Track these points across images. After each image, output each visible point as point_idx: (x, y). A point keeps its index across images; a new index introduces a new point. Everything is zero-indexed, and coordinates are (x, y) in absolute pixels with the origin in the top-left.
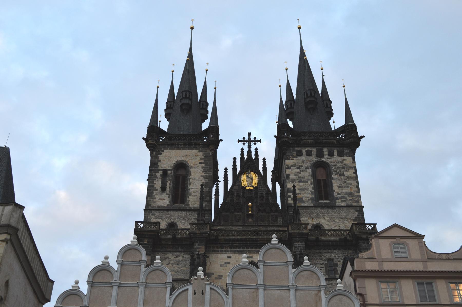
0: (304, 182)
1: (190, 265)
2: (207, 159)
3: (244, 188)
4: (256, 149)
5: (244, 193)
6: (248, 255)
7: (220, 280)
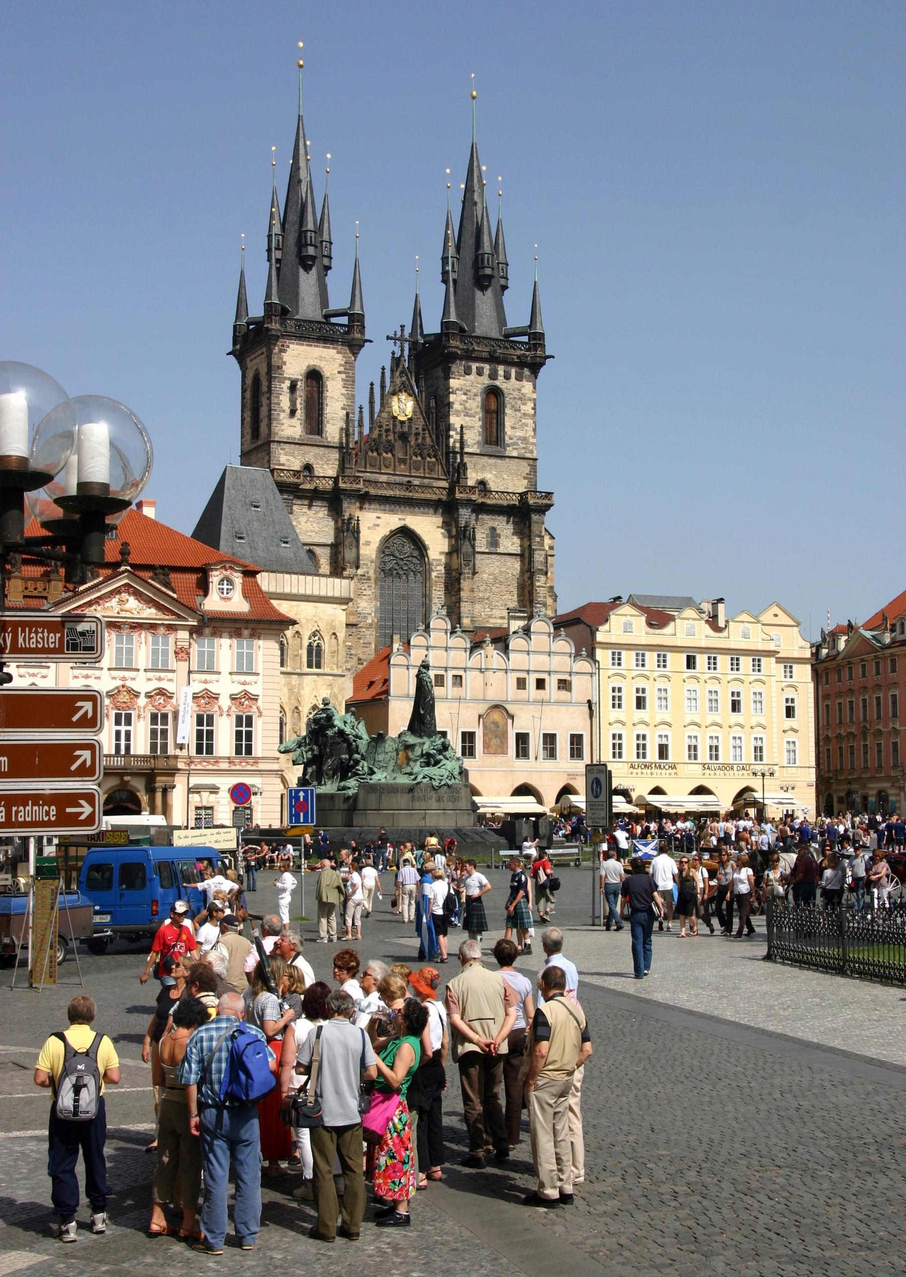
3: (395, 418)
5: (394, 426)
6: (400, 517)
7: (368, 547)
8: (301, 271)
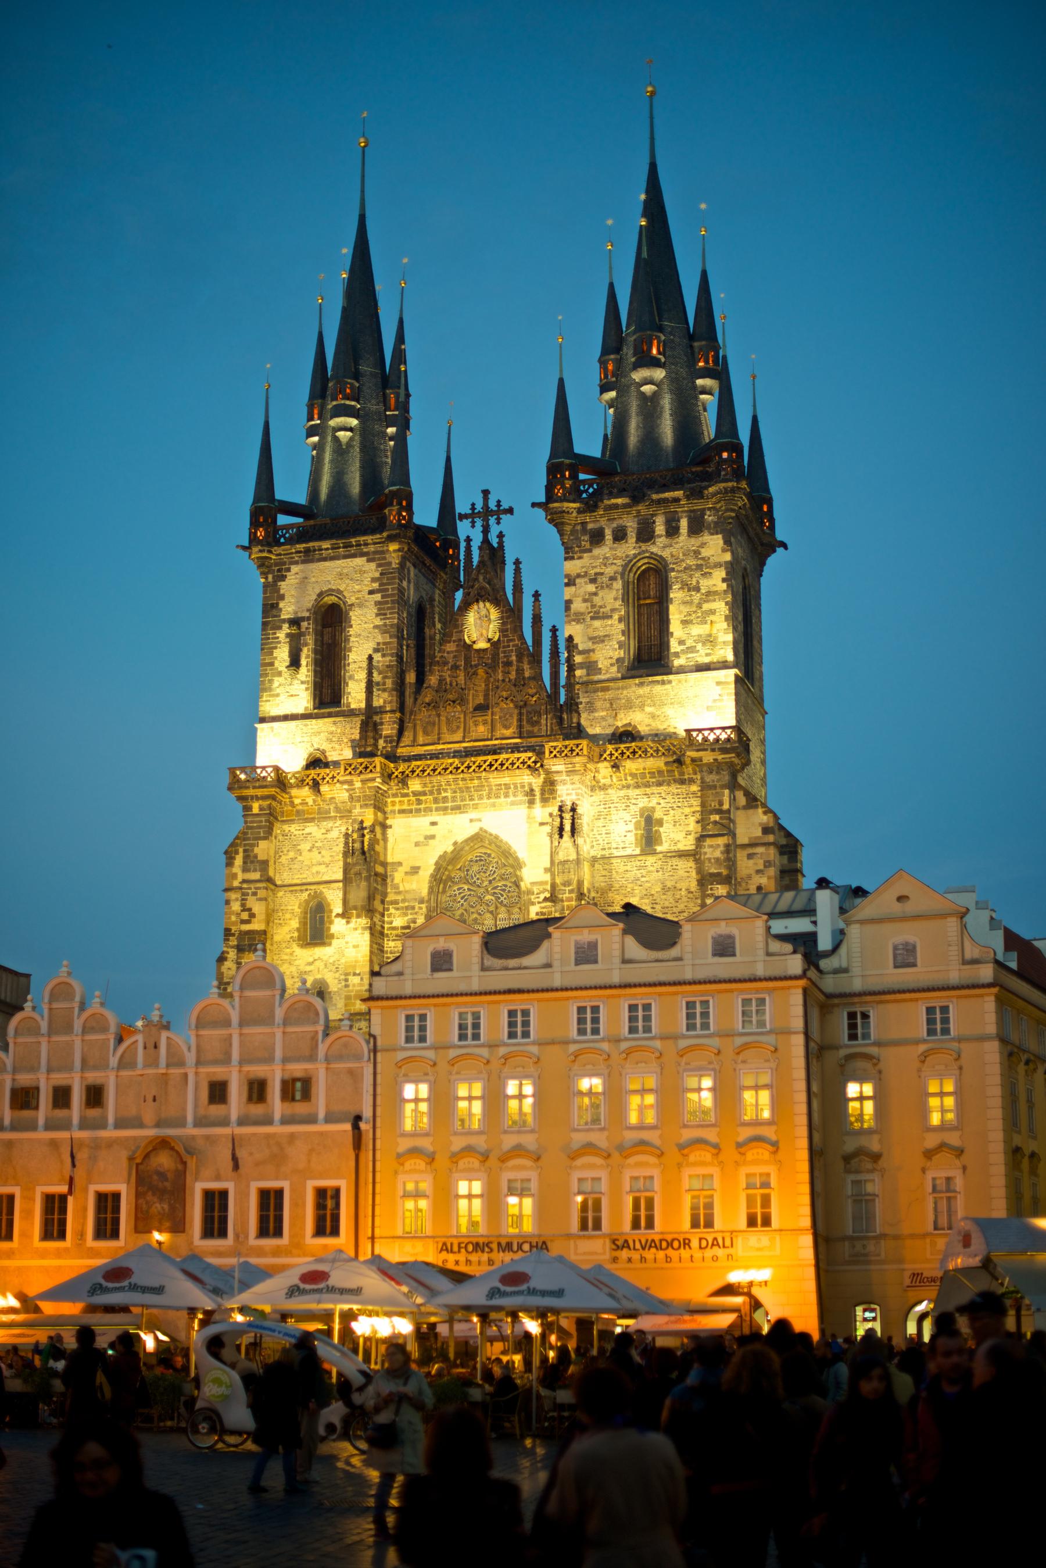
1: (346, 854)
2: (385, 581)
4: (501, 536)
5: (467, 660)
6: (473, 814)
7: (415, 877)
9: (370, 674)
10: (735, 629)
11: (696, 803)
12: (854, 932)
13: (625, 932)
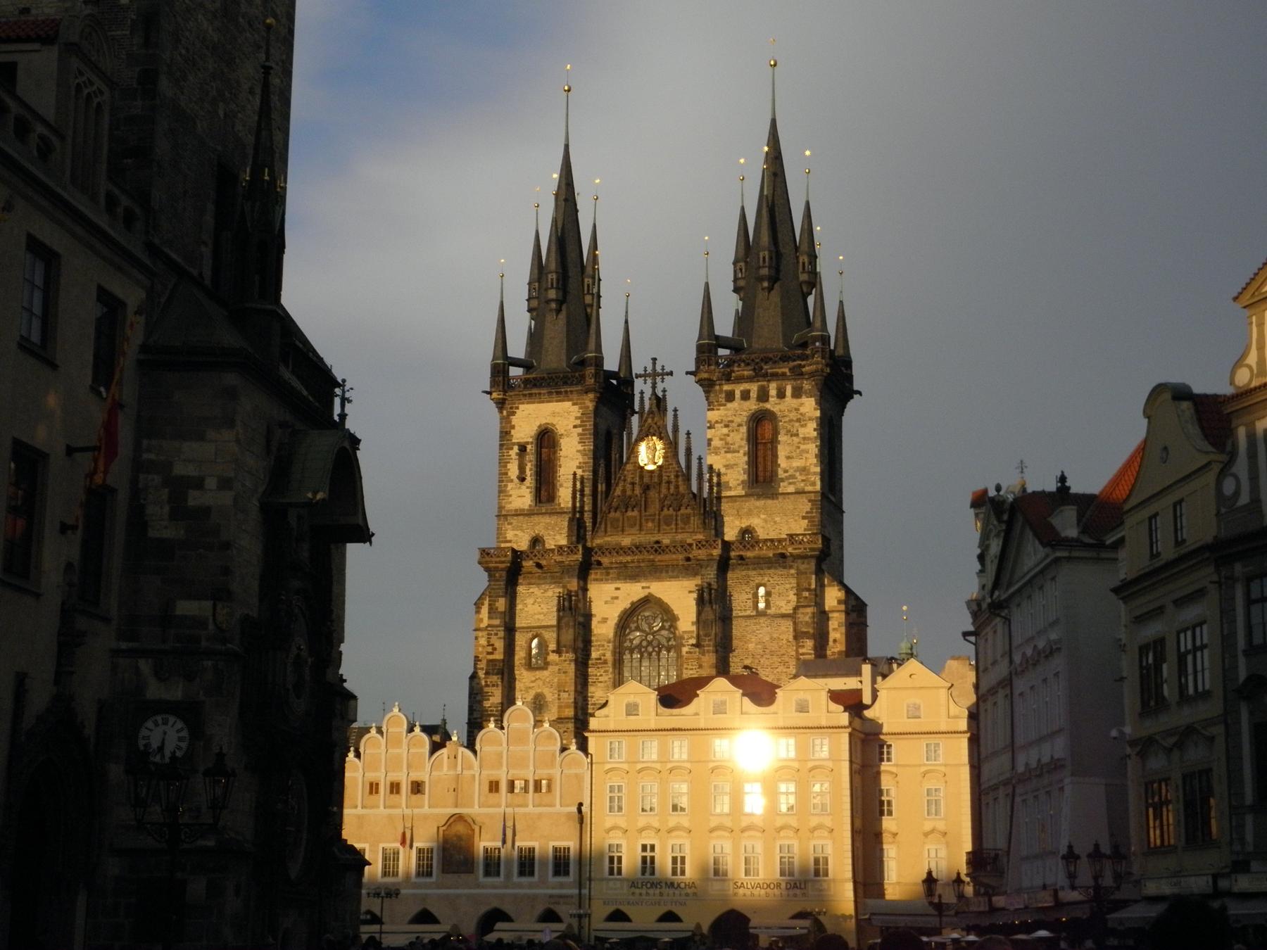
0: (734, 452)
1: (559, 611)
4: (664, 391)
5: (641, 477)
6: (644, 584)
8: (550, 317)
9: (574, 485)
10: (822, 463)
11: (794, 581)
12: (882, 695)
13: (743, 695)
